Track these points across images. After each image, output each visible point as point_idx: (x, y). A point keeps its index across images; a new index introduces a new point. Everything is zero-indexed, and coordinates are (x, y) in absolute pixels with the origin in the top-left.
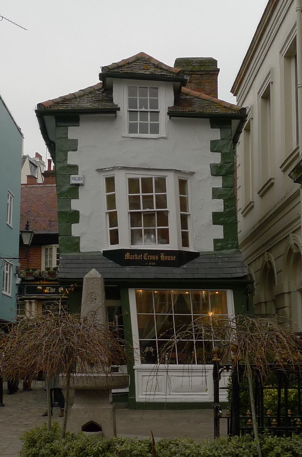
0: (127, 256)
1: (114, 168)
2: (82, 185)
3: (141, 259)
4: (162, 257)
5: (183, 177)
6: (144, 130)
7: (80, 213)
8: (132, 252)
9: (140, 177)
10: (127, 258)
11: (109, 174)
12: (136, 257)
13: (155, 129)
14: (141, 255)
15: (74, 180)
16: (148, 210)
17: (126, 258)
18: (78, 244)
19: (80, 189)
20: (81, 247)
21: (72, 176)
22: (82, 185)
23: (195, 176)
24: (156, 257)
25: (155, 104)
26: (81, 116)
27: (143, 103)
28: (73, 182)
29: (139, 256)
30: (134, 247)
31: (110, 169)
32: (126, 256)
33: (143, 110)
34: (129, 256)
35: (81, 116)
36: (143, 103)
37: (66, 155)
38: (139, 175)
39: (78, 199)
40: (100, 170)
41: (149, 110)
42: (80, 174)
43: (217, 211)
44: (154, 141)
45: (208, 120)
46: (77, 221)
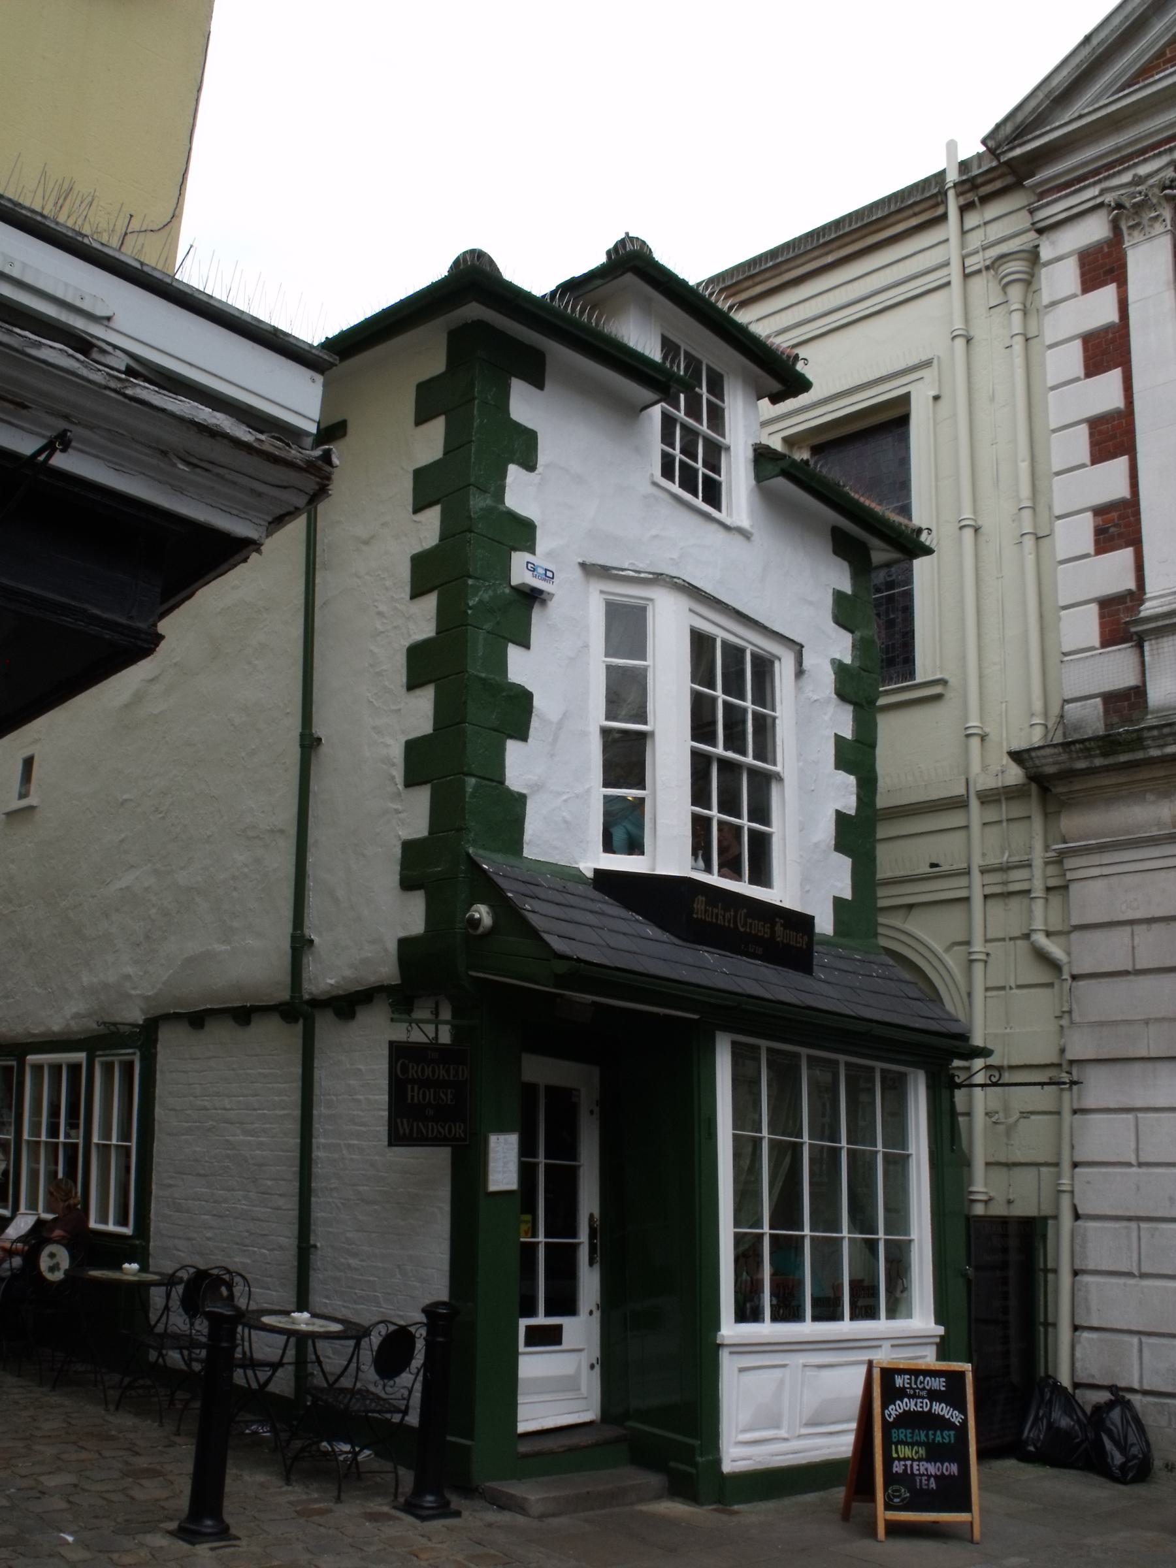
1: (657, 579)
3: (732, 925)
6: (689, 483)
7: (536, 702)
9: (720, 634)
10: (699, 916)
13: (713, 494)
14: (732, 913)
15: (521, 571)
17: (697, 913)
20: (527, 837)
24: (764, 926)
25: (717, 418)
29: (727, 915)
31: (642, 575)
32: (695, 906)
34: (703, 907)
38: (722, 630)
43: (845, 811)
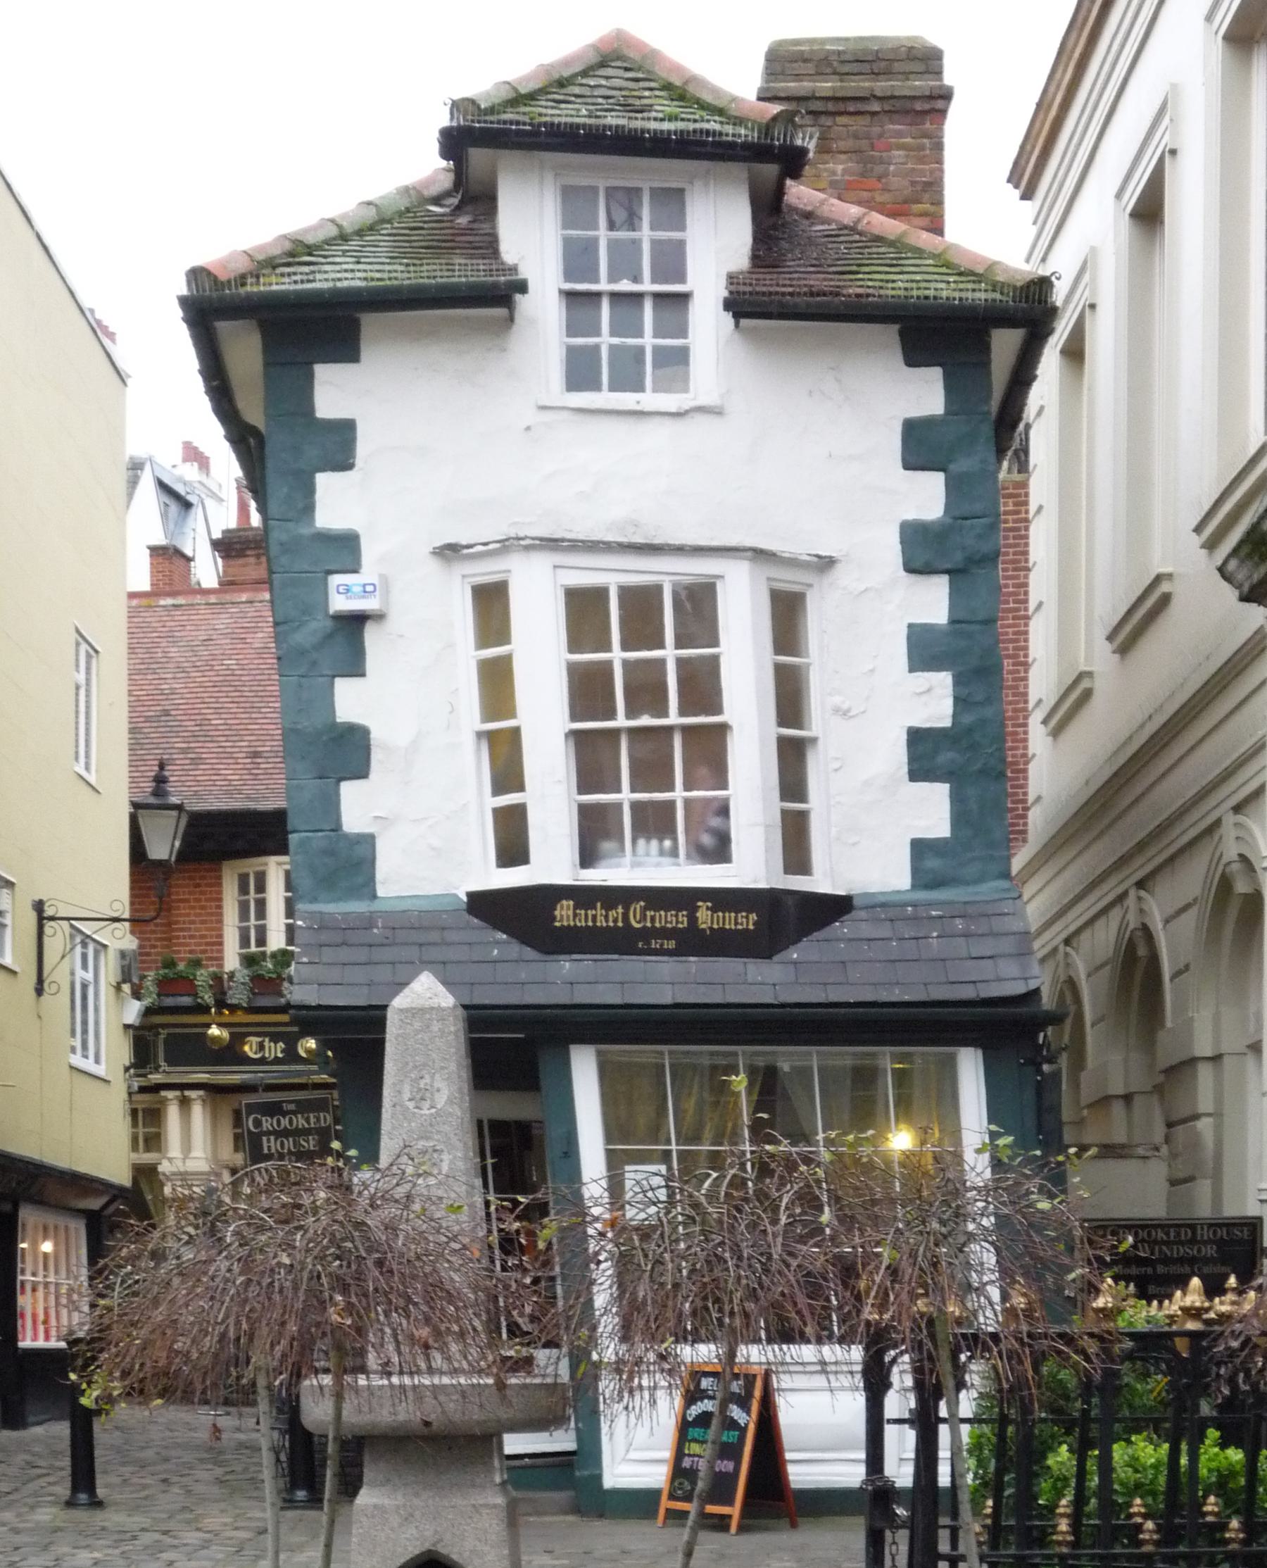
0: (564, 913)
2: (379, 617)
4: (705, 917)
5: (789, 580)
8: (584, 896)
11: (486, 572)
12: (601, 917)
16: (646, 721)
18: (368, 863)
19: (372, 636)
20: (379, 876)
21: (336, 580)
22: (379, 617)
23: (839, 570)
26: (370, 322)
27: (625, 262)
28: (339, 603)
30: (595, 877)
33: (625, 286)
35: (370, 322)
36: (625, 262)
37: (310, 490)
39: (363, 675)
40: (450, 552)
41: (647, 286)
42: (370, 571)
44: (669, 425)
45: (894, 329)
46: (361, 772)
